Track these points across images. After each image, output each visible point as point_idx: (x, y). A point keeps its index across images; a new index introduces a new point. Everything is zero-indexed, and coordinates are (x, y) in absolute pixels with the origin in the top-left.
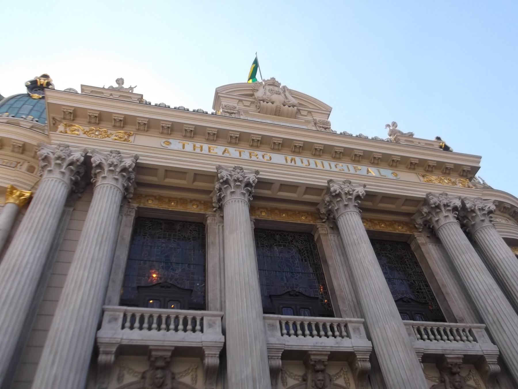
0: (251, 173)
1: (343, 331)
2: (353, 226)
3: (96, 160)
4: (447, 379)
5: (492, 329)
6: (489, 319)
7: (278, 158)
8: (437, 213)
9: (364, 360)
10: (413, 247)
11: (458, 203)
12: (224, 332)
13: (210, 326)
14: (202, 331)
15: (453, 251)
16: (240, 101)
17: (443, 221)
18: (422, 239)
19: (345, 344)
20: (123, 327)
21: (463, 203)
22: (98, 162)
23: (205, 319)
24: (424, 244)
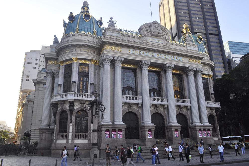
0: (149, 61)
1: (163, 100)
2: (170, 75)
3: (116, 58)
4: (180, 109)
7: (155, 55)
8: (189, 72)
9: (166, 106)
10: (182, 77)
11: (195, 69)
12: (142, 100)
13: (140, 99)
14: (138, 100)
15: (190, 83)
16: (147, 31)
17: (190, 74)
18: (184, 76)
19: (163, 103)
20: (125, 99)
21: (196, 68)
22: (116, 60)
23: (139, 97)
24: (184, 77)
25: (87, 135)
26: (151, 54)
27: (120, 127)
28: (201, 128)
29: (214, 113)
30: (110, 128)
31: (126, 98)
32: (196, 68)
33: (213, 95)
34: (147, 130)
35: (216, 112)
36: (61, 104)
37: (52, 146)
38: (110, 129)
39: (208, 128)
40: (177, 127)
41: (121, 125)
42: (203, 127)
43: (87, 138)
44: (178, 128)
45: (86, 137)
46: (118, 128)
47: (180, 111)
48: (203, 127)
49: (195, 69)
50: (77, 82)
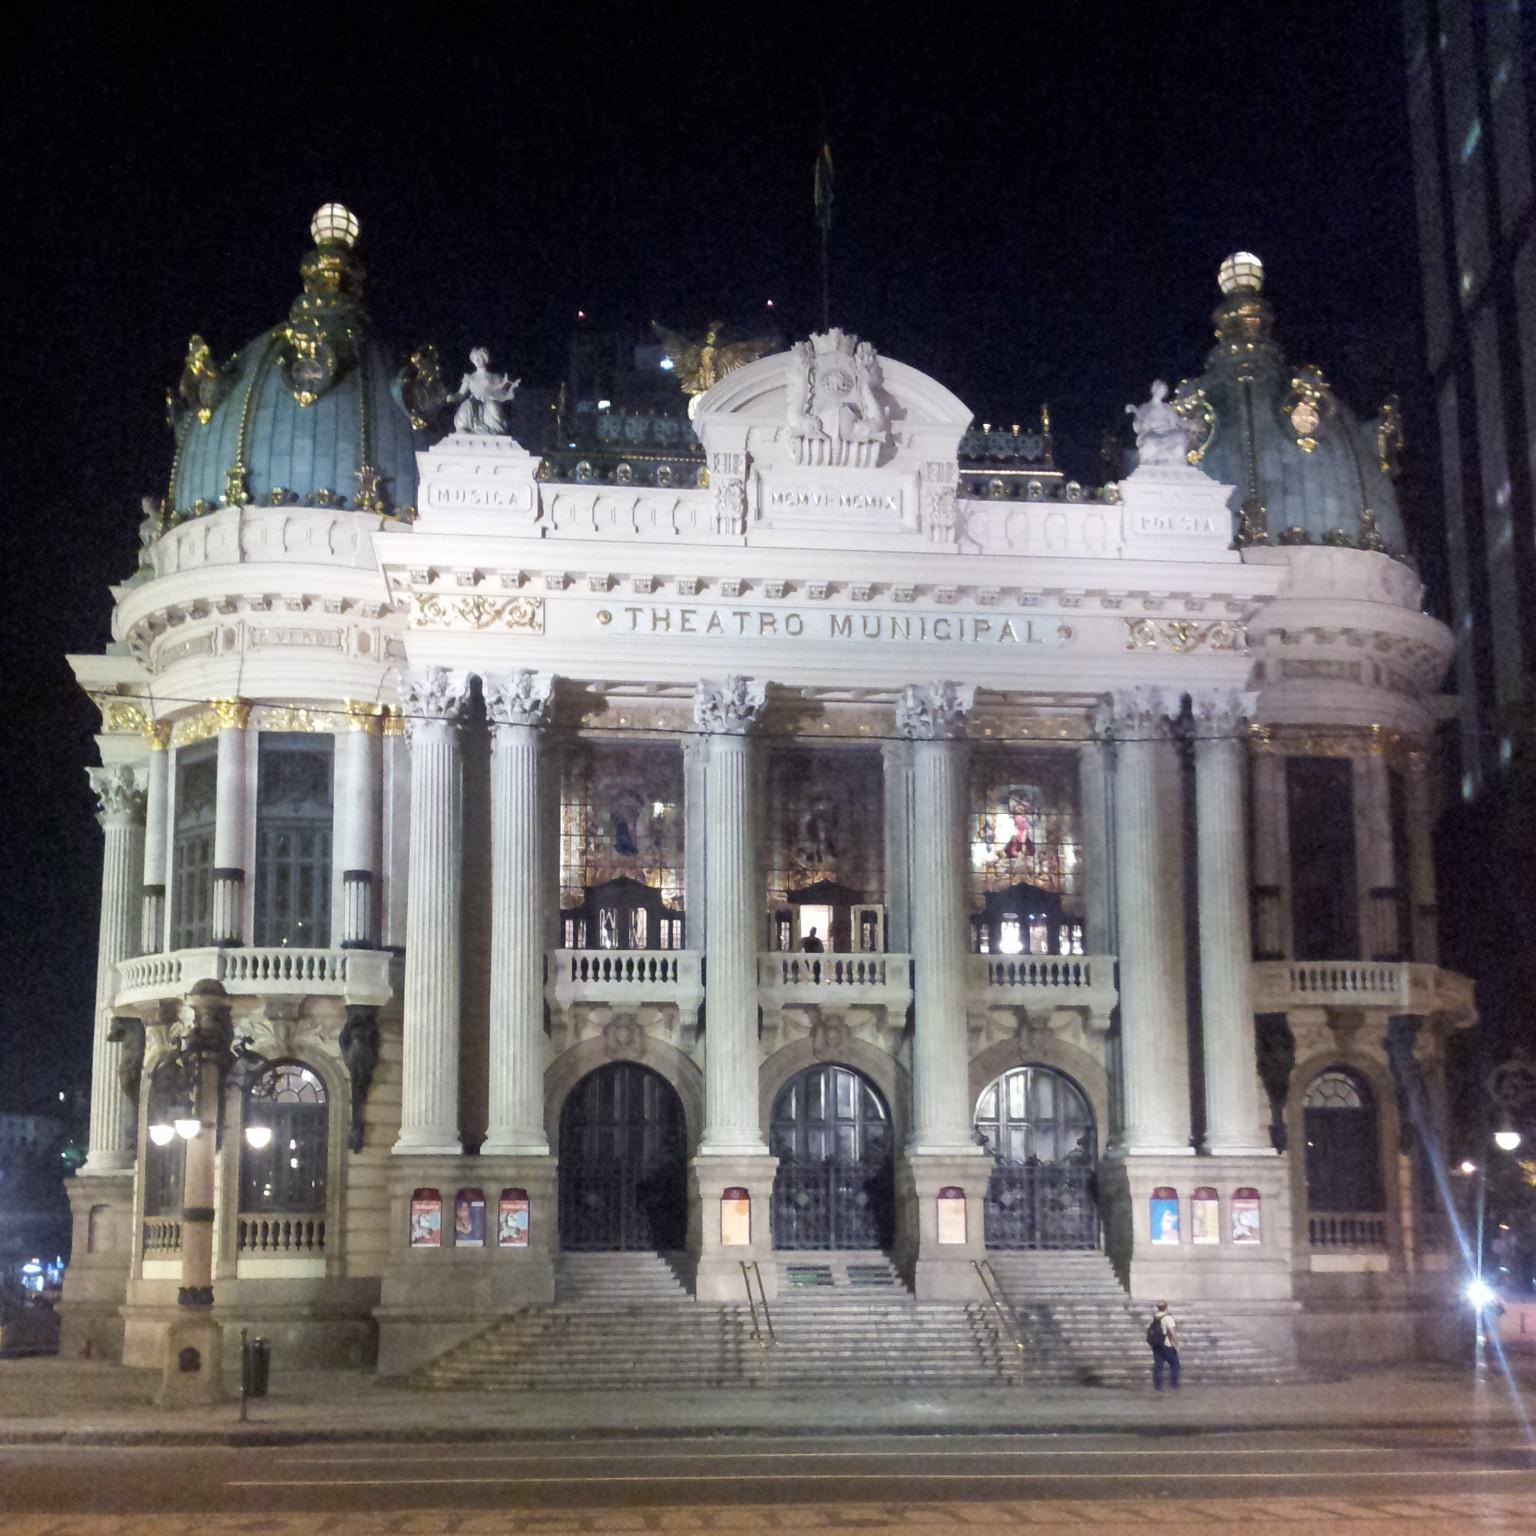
4: (1024, 1033)
5: (1123, 969)
6: (1123, 951)
9: (897, 1015)
13: (687, 970)
14: (675, 978)
19: (875, 994)
21: (1186, 702)
25: (322, 1227)
26: (781, 625)
27: (510, 1172)
28: (1169, 1179)
29: (1362, 1055)
30: (442, 1179)
31: (579, 973)
32: (1186, 702)
33: (1387, 906)
34: (718, 1188)
35: (1387, 1045)
36: (155, 1024)
37: (129, 1297)
38: (445, 1189)
39: (1238, 1179)
40: (952, 1171)
41: (520, 1160)
42: (1192, 1172)
43: (321, 1244)
44: (965, 1177)
45: (315, 1239)
46: (496, 1179)
47: (1025, 1046)
48: (1192, 1172)
49: (1173, 708)
50: (251, 871)
